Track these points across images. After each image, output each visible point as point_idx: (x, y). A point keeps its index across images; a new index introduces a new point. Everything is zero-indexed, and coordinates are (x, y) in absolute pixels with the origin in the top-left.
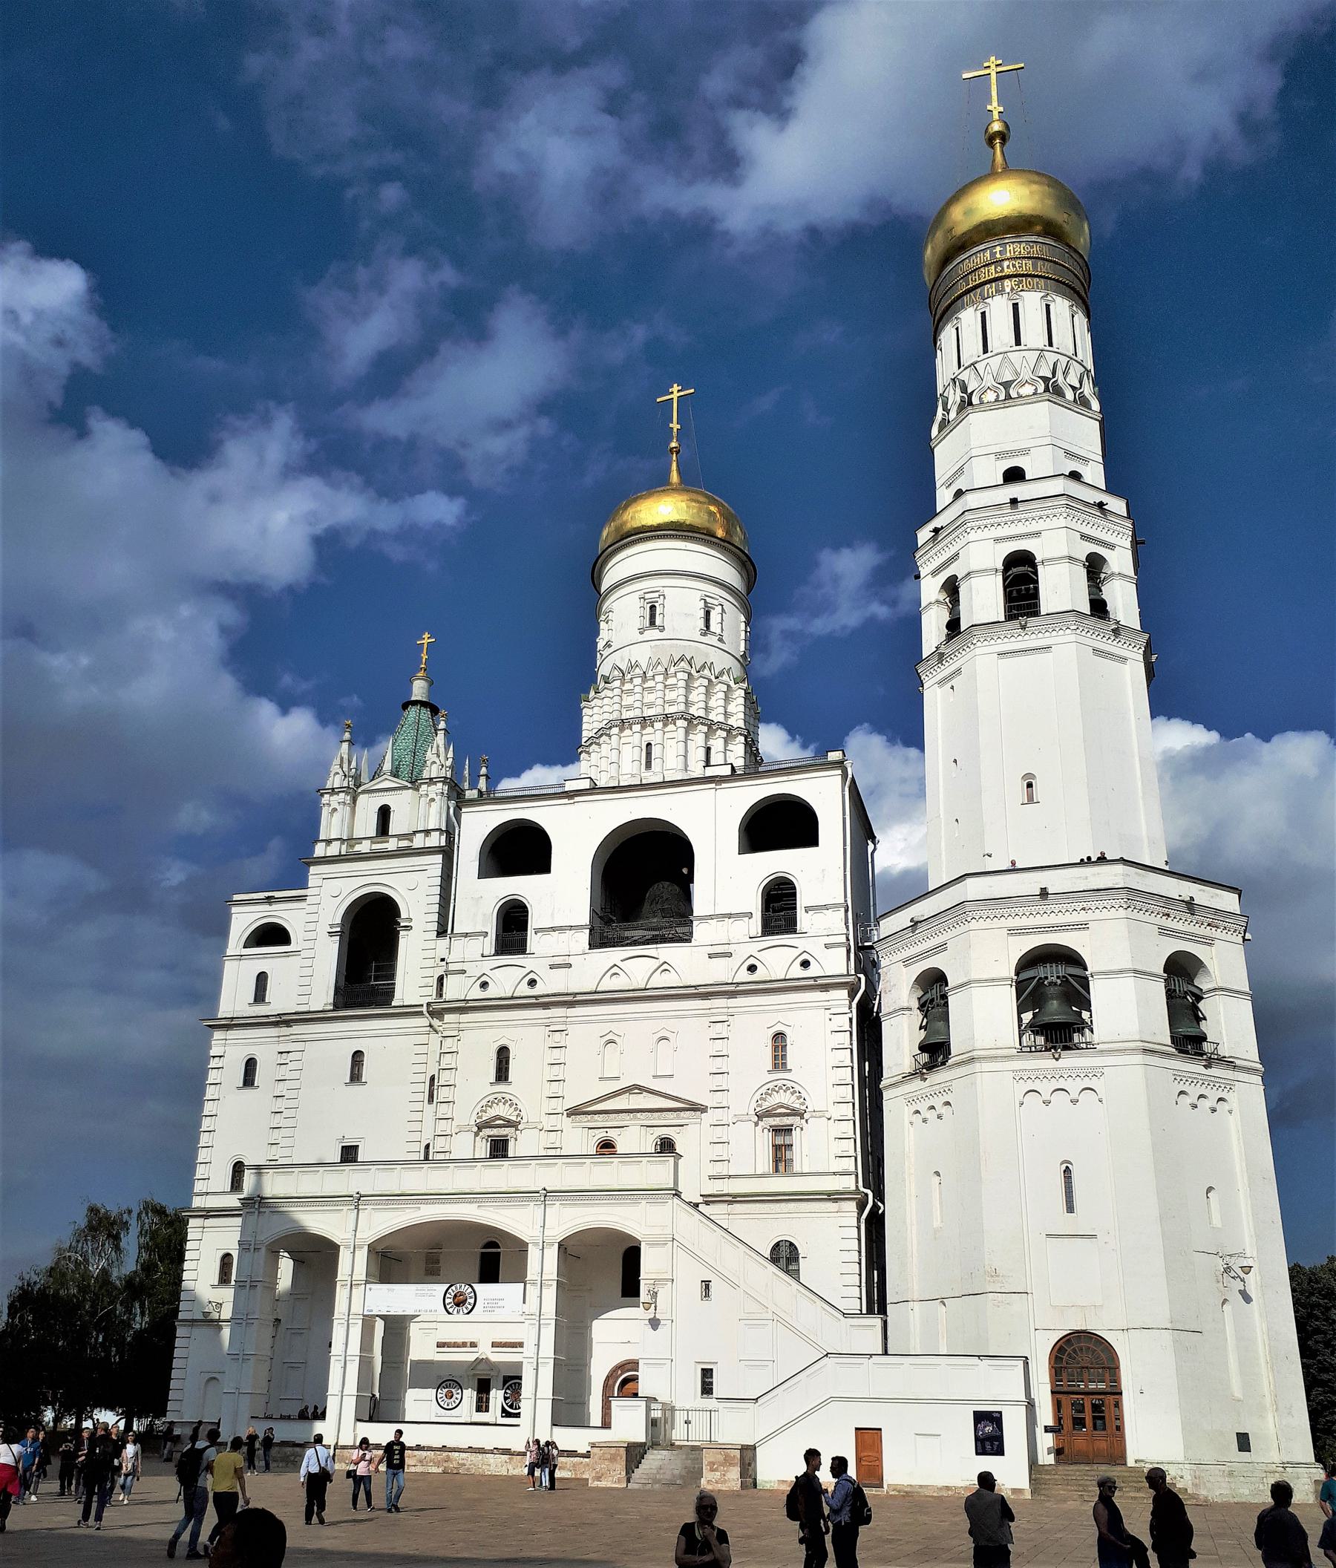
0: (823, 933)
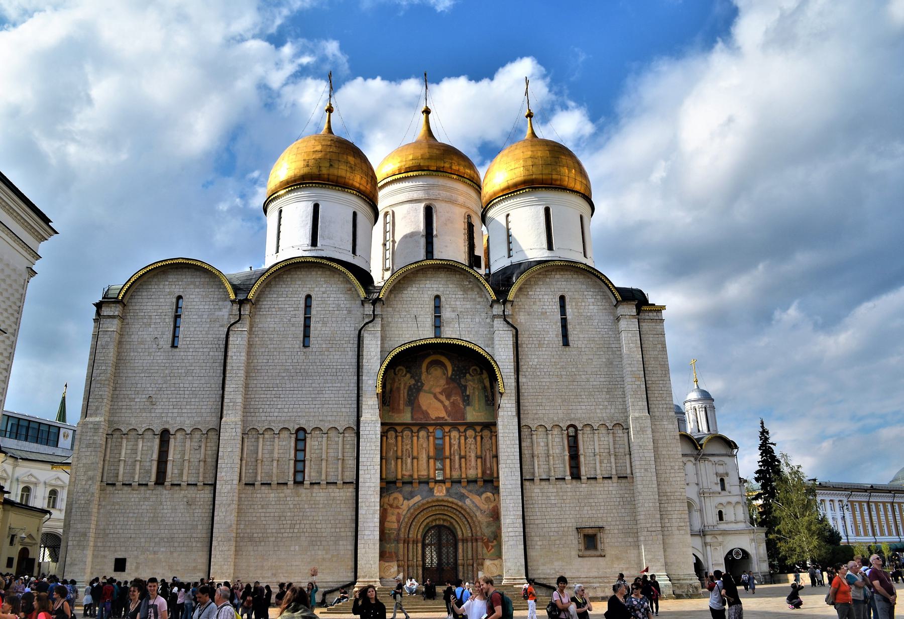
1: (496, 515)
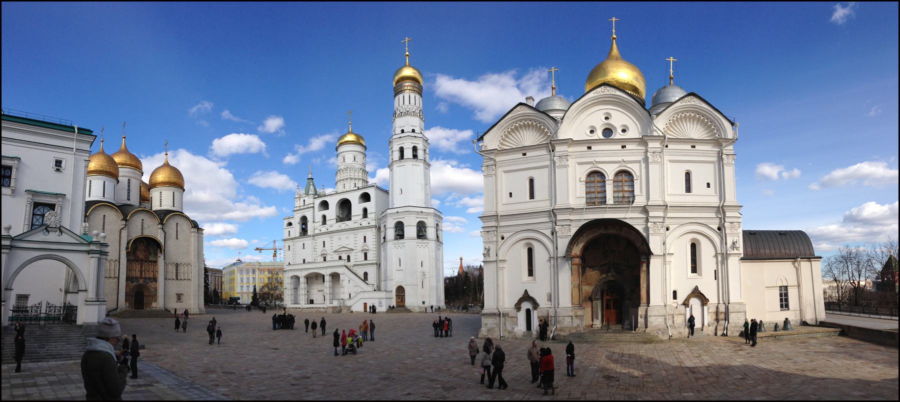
0: (372, 219)
1: (156, 289)
